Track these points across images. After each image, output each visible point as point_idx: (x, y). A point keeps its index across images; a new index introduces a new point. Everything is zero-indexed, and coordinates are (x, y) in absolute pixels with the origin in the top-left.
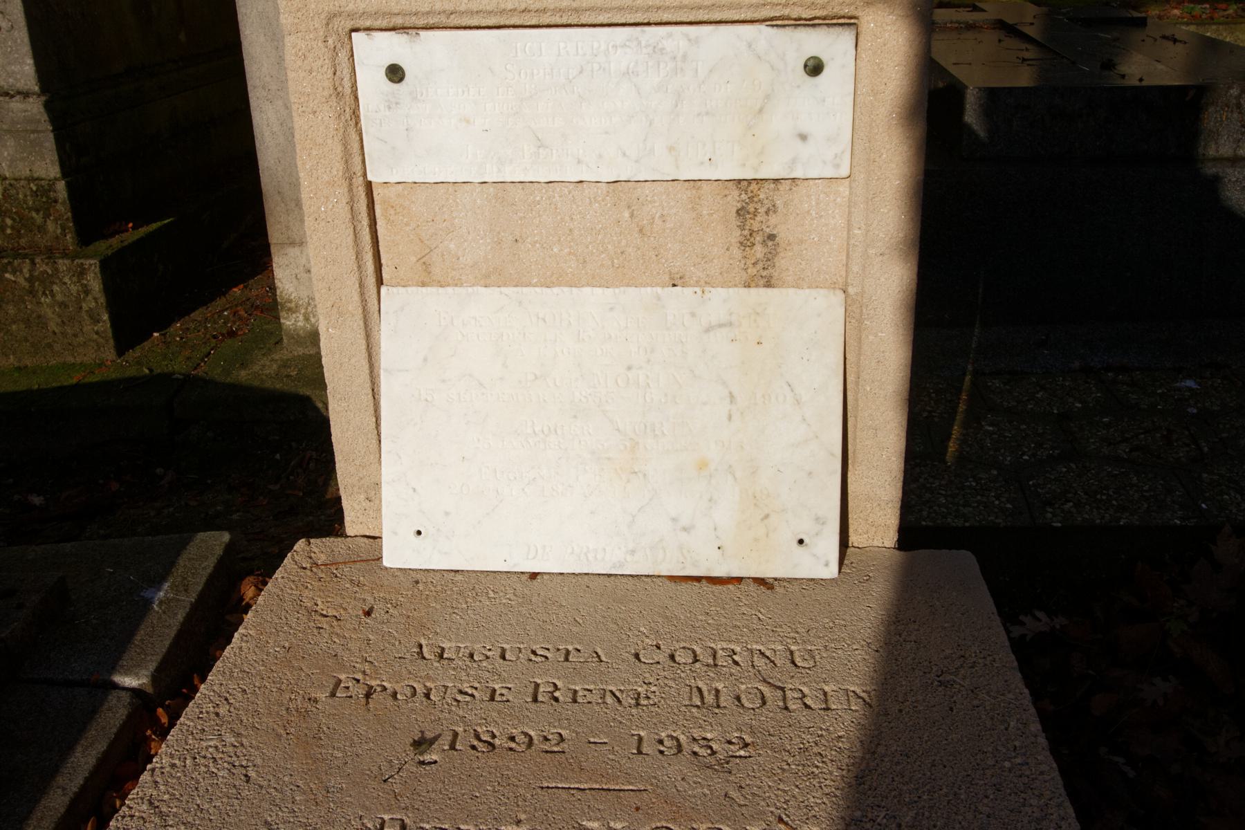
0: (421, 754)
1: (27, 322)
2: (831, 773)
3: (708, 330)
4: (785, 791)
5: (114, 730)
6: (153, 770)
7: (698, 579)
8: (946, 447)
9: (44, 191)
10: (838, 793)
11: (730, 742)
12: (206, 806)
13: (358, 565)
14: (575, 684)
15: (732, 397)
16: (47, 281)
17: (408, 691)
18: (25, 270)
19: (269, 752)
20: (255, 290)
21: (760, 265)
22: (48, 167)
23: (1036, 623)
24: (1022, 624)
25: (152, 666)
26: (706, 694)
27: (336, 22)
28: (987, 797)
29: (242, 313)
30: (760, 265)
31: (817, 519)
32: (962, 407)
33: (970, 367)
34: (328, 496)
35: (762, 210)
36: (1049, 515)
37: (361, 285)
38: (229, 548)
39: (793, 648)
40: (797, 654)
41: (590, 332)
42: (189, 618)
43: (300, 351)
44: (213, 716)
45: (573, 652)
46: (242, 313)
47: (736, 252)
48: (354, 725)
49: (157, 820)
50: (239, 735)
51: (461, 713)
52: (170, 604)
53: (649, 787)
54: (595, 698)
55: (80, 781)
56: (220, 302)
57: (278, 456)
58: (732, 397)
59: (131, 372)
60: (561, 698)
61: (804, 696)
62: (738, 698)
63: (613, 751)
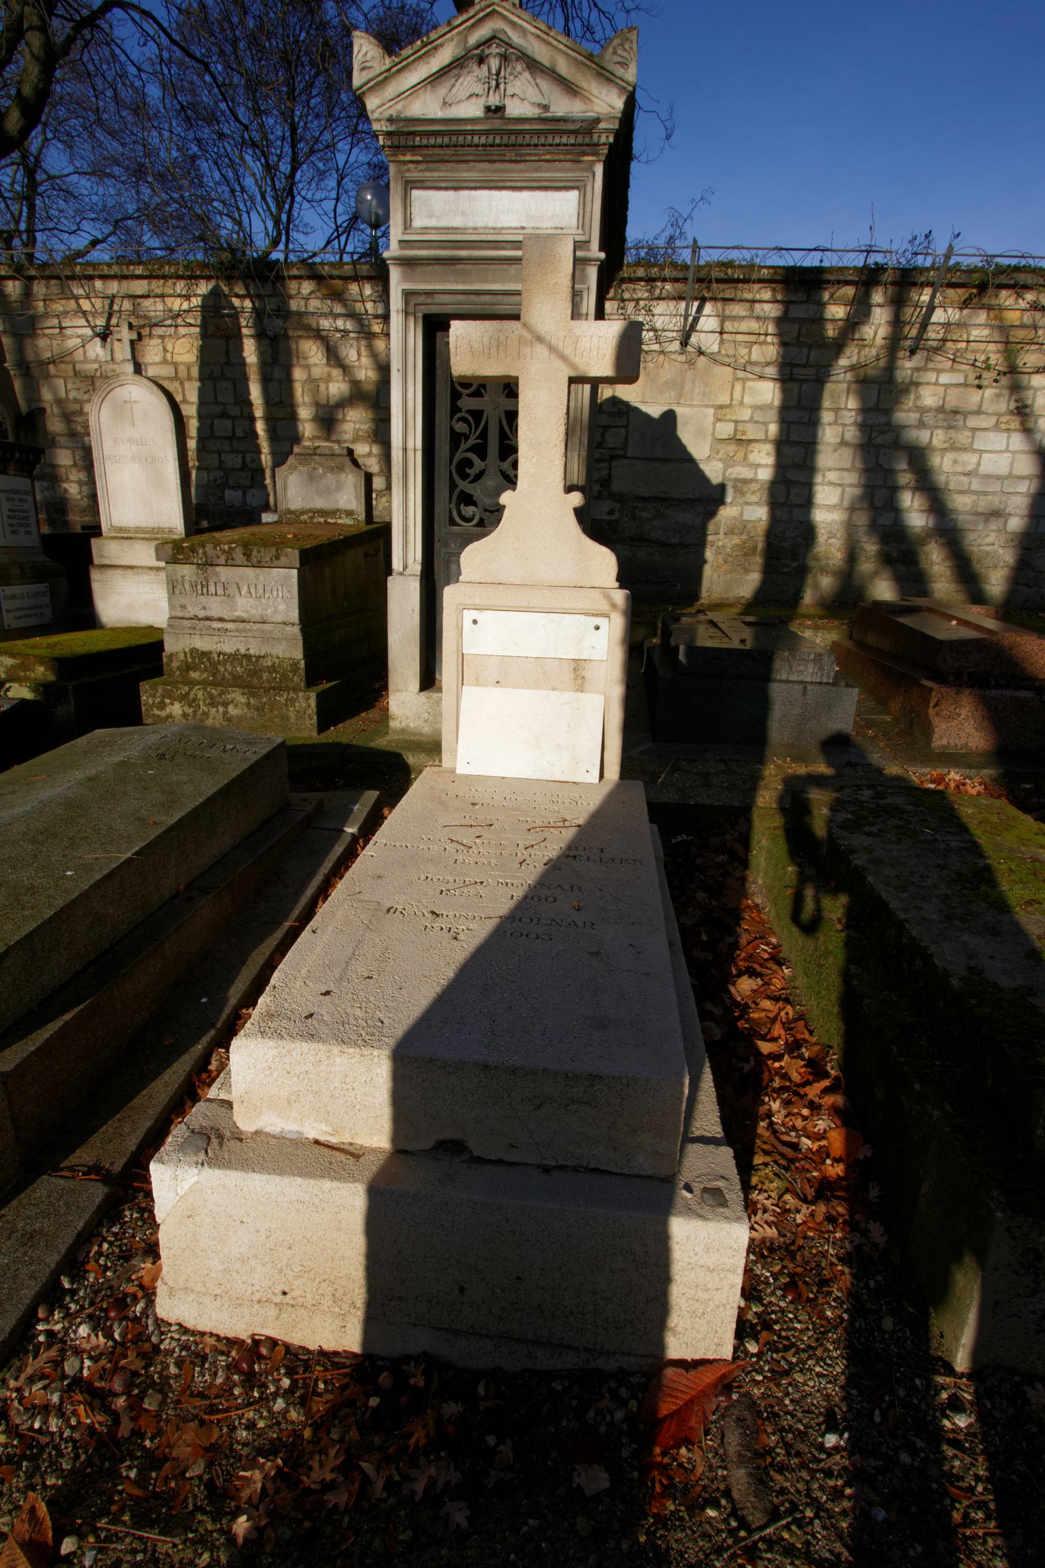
1: (282, 718)
9: (295, 664)
16: (293, 701)
20: (373, 714)
22: (298, 654)
38: (379, 797)
52: (361, 809)
56: (356, 719)
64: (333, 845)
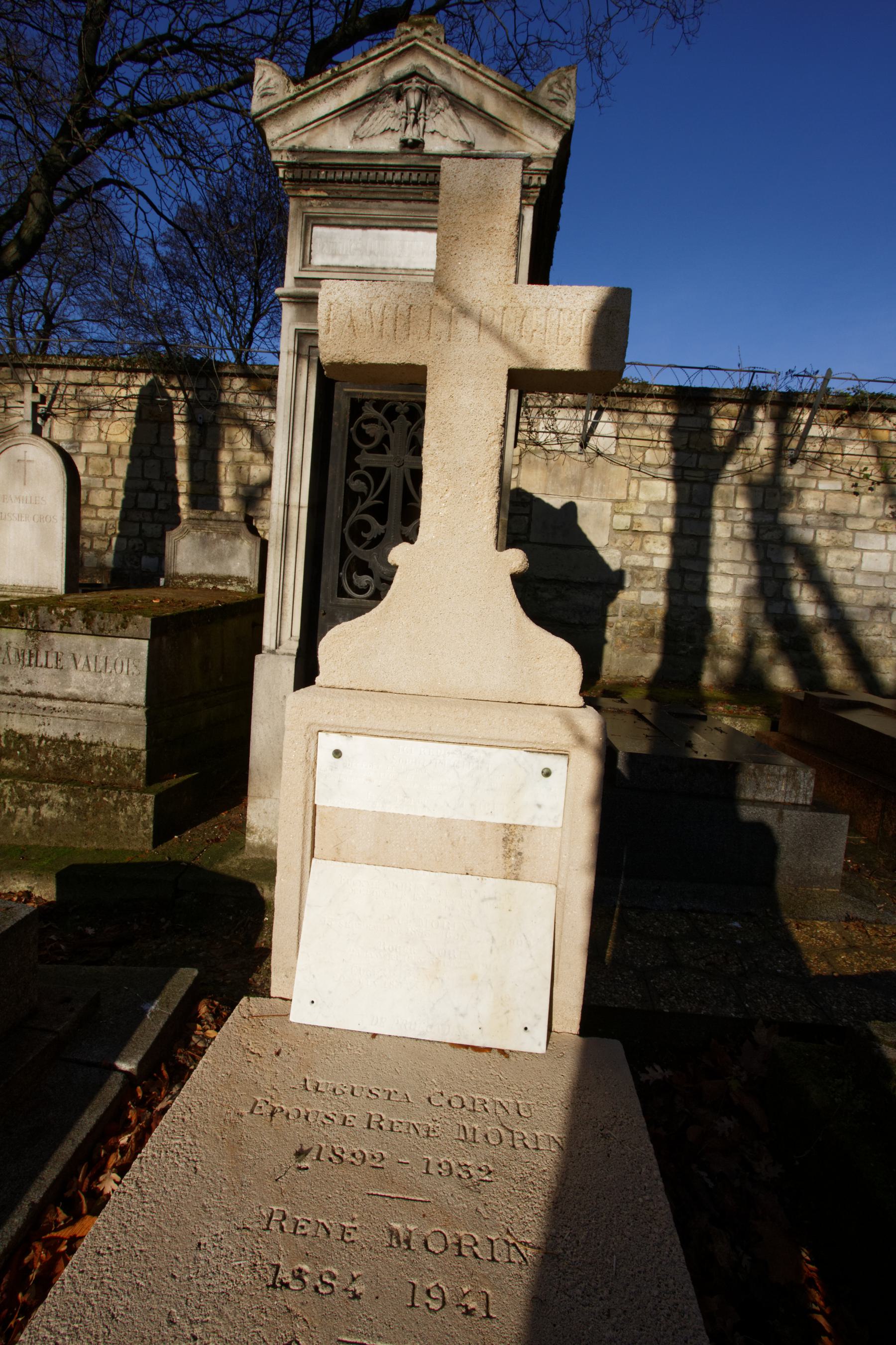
0: (300, 1161)
1: (109, 825)
2: (538, 1198)
3: (483, 900)
4: (511, 1210)
5: (110, 1100)
6: (141, 1158)
7: (467, 1047)
8: (605, 953)
9: (134, 756)
10: (542, 1214)
11: (480, 1169)
12: (169, 1189)
13: (275, 1018)
14: (392, 1117)
15: (493, 940)
16: (124, 804)
17: (296, 1113)
18: (115, 797)
19: (211, 1152)
20: (234, 815)
21: (513, 868)
22: (140, 743)
23: (655, 1073)
24: (647, 1072)
25: (140, 1057)
26: (468, 1131)
27: (312, 727)
28: (629, 1224)
29: (225, 828)
30: (513, 868)
31: (536, 1016)
32: (614, 928)
33: (618, 903)
34: (256, 946)
35: (516, 840)
36: (662, 1004)
37: (303, 858)
38: (197, 980)
39: (519, 1102)
40: (521, 1106)
41: (422, 894)
42: (167, 1024)
43: (254, 856)
44: (181, 1121)
45: (393, 1093)
46: (225, 828)
47: (501, 859)
48: (262, 1136)
49: (139, 1197)
50: (194, 1137)
51: (325, 1132)
53: (432, 1200)
54: (403, 1128)
55: (84, 1135)
56: (214, 820)
57: (231, 918)
58: (493, 940)
59: (159, 858)
60: (384, 1127)
61: (524, 1138)
62: (486, 1136)
63: (412, 1170)
64: (80, 1111)
